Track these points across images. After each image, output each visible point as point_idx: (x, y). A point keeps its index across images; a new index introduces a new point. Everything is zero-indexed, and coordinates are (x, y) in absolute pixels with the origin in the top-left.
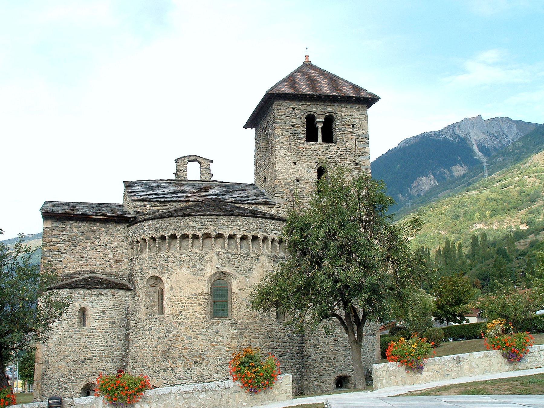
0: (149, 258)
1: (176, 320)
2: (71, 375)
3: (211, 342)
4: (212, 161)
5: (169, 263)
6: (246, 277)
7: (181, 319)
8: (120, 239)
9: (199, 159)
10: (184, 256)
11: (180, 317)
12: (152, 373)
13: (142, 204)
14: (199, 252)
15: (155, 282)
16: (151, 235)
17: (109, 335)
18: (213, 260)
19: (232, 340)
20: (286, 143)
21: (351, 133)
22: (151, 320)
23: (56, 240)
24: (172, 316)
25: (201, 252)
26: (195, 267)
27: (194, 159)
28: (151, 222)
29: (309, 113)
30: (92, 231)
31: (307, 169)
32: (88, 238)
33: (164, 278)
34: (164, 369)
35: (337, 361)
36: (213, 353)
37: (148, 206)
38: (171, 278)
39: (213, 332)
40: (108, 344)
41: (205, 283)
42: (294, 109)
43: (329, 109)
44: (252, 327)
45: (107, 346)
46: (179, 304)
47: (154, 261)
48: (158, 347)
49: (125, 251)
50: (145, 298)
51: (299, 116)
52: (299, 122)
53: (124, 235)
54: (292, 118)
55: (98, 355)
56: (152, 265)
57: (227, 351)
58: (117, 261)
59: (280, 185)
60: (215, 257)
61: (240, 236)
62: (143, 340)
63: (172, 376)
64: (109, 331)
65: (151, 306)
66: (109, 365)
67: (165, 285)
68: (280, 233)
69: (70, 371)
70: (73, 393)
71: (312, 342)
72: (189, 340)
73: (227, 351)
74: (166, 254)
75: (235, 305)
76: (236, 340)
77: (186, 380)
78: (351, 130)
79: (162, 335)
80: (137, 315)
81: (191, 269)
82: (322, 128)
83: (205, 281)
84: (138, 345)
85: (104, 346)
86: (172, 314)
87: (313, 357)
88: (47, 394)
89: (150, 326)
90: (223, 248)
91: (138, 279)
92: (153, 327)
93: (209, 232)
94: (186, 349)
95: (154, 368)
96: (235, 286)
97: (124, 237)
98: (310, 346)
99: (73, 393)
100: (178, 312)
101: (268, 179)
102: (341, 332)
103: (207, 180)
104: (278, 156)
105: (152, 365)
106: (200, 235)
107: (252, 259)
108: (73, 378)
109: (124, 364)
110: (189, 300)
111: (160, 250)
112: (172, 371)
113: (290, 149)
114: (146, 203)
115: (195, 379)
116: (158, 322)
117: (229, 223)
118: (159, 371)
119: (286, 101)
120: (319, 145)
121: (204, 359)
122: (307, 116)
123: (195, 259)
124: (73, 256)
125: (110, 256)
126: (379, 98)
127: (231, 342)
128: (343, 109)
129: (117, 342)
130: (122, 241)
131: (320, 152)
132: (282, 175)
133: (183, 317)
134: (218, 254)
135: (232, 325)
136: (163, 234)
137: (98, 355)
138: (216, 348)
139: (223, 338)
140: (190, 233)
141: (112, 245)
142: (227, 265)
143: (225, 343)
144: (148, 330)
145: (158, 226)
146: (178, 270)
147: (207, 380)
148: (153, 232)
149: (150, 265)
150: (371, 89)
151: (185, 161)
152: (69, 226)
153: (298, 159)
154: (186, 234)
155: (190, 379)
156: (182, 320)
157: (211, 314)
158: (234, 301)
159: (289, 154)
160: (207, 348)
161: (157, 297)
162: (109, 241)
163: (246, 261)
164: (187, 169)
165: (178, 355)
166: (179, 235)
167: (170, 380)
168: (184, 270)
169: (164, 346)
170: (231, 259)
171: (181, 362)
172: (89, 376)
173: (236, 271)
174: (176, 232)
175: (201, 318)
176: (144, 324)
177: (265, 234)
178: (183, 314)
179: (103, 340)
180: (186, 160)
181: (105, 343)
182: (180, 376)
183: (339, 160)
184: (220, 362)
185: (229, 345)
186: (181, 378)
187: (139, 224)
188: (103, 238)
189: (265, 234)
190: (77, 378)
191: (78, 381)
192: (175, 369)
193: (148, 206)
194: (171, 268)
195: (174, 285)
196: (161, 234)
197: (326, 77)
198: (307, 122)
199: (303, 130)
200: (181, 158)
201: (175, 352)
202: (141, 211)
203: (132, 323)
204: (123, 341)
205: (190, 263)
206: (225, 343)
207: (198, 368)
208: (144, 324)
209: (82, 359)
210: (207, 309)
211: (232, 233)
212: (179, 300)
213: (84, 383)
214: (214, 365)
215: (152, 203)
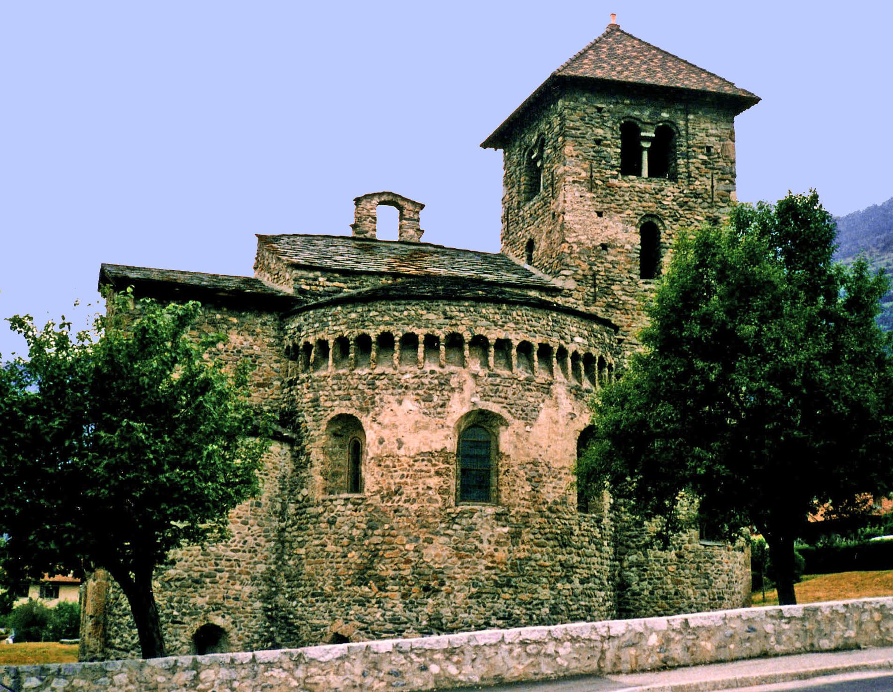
0: (333, 379)
1: (389, 504)
2: (172, 607)
3: (457, 549)
4: (422, 207)
5: (376, 391)
7: (399, 501)
8: (267, 340)
9: (401, 203)
10: (408, 376)
12: (334, 609)
13: (311, 275)
14: (438, 369)
15: (343, 428)
16: (340, 333)
17: (249, 529)
18: (465, 387)
20: (584, 174)
21: (704, 162)
22: (335, 503)
24: (378, 497)
25: (441, 370)
26: (428, 399)
27: (393, 200)
28: (339, 308)
29: (627, 120)
31: (621, 226)
33: (365, 420)
34: (361, 601)
35: (682, 598)
36: (460, 571)
37: (321, 279)
38: (379, 419)
39: (463, 529)
40: (246, 548)
41: (449, 433)
42: (600, 110)
43: (665, 115)
44: (536, 521)
45: (244, 551)
46: (396, 471)
47: (345, 384)
48: (349, 555)
49: (275, 366)
50: (322, 458)
51: (609, 124)
52: (609, 136)
53: (274, 333)
54: (597, 127)
55: (227, 569)
56: (341, 392)
57: (488, 568)
58: (259, 385)
59: (571, 253)
60: (470, 383)
61: (516, 343)
62: (317, 542)
63: (378, 615)
64: (251, 521)
66: (247, 590)
67: (367, 433)
68: (586, 342)
69: (171, 600)
70: (175, 643)
71: (633, 558)
72: (414, 544)
73: (488, 568)
74: (370, 371)
75: (505, 479)
76: (506, 548)
77: (406, 623)
78: (705, 158)
79: (355, 532)
80: (304, 492)
81: (423, 403)
82: (649, 150)
83: (448, 427)
84: (302, 551)
85: (239, 551)
86: (379, 492)
87: (635, 587)
88: (120, 644)
89: (332, 514)
90: (485, 364)
91: (306, 419)
93: (460, 332)
94: (408, 561)
95: (339, 599)
96: (506, 440)
97: (274, 337)
98: (630, 567)
99: (175, 643)
101: (542, 245)
102: (690, 542)
103: (412, 241)
104: (569, 197)
105: (335, 593)
106: (442, 337)
107: (538, 390)
108: (175, 613)
109: (274, 589)
110: (416, 464)
111: (357, 364)
112: (376, 605)
113: (591, 185)
114: (318, 273)
115: (424, 623)
116: (350, 506)
117: (498, 317)
118: (349, 605)
119: (587, 95)
120: (642, 182)
121: (442, 584)
122: (622, 125)
123: (430, 383)
126: (760, 99)
127: (496, 550)
128: (691, 117)
129: (263, 543)
130: (270, 345)
131: (647, 196)
132: (574, 234)
133: (404, 498)
134: (475, 376)
135: (498, 517)
136: (366, 331)
137: (227, 569)
138: (468, 562)
139: (481, 542)
140: (421, 333)
141: (251, 351)
142: (493, 399)
143: (485, 553)
145: (353, 315)
147: (449, 625)
148: (343, 327)
149: (337, 393)
150: (743, 83)
151: (374, 202)
153: (606, 206)
154: (413, 334)
155: (415, 622)
156: (400, 503)
157: (458, 493)
158: (503, 470)
159: (589, 195)
160: (449, 561)
161: (344, 459)
162: (245, 343)
163: (527, 393)
164: (375, 218)
165: (391, 573)
166: (398, 335)
167: (372, 623)
168: (409, 403)
169: (361, 556)
170: (500, 388)
171: (397, 588)
172: (207, 612)
173: (509, 412)
174: (392, 328)
175: (440, 499)
176: (321, 509)
177: (562, 342)
179: (238, 540)
180: (376, 201)
181: (241, 544)
182: (394, 615)
183: (681, 212)
184: (474, 590)
185: (492, 556)
186: (395, 620)
187: (311, 312)
188: (235, 339)
189: (562, 342)
190: (184, 614)
191: (186, 619)
192: (383, 600)
193: (321, 279)
194: (381, 400)
195: (386, 433)
197: (654, 55)
198: (622, 138)
199: (614, 151)
200: (366, 196)
201: (384, 569)
202: (308, 288)
203: (292, 509)
204: (272, 544)
205: (421, 392)
206: (485, 553)
207: (430, 601)
208: (321, 509)
209: (196, 575)
210: (453, 483)
211: (502, 336)
212: (397, 464)
213: (198, 625)
214: (461, 595)
215: (329, 274)
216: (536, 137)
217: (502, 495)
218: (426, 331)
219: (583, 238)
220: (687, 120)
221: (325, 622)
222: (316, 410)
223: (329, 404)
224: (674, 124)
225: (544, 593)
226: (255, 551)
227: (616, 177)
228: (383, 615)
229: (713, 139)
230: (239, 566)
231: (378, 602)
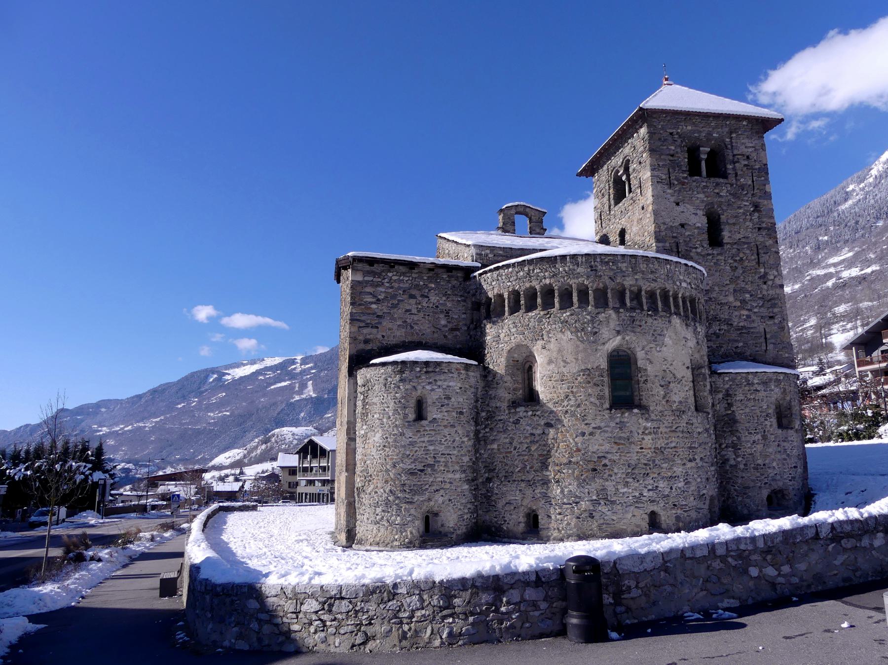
1: (560, 409)
6: (657, 345)
11: (566, 403)
19: (645, 437)
21: (745, 165)
23: (369, 299)
30: (417, 287)
32: (412, 297)
40: (456, 444)
42: (671, 134)
49: (464, 316)
65: (514, 390)
66: (458, 476)
73: (637, 452)
82: (707, 161)
84: (495, 446)
97: (461, 296)
114: (488, 251)
120: (702, 181)
124: (393, 319)
125: (443, 322)
146: (560, 335)
152: (386, 280)
156: (568, 408)
158: (642, 380)
159: (669, 191)
164: (514, 223)
180: (513, 212)
196: (528, 285)
199: (683, 159)
216: (621, 160)
217: (644, 400)
218: (576, 281)
219: (668, 220)
223: (507, 339)
224: (724, 141)
225: (679, 470)
226: (461, 447)
227: (686, 178)
228: (562, 492)
229: (750, 150)
230: (451, 458)
231: (558, 482)
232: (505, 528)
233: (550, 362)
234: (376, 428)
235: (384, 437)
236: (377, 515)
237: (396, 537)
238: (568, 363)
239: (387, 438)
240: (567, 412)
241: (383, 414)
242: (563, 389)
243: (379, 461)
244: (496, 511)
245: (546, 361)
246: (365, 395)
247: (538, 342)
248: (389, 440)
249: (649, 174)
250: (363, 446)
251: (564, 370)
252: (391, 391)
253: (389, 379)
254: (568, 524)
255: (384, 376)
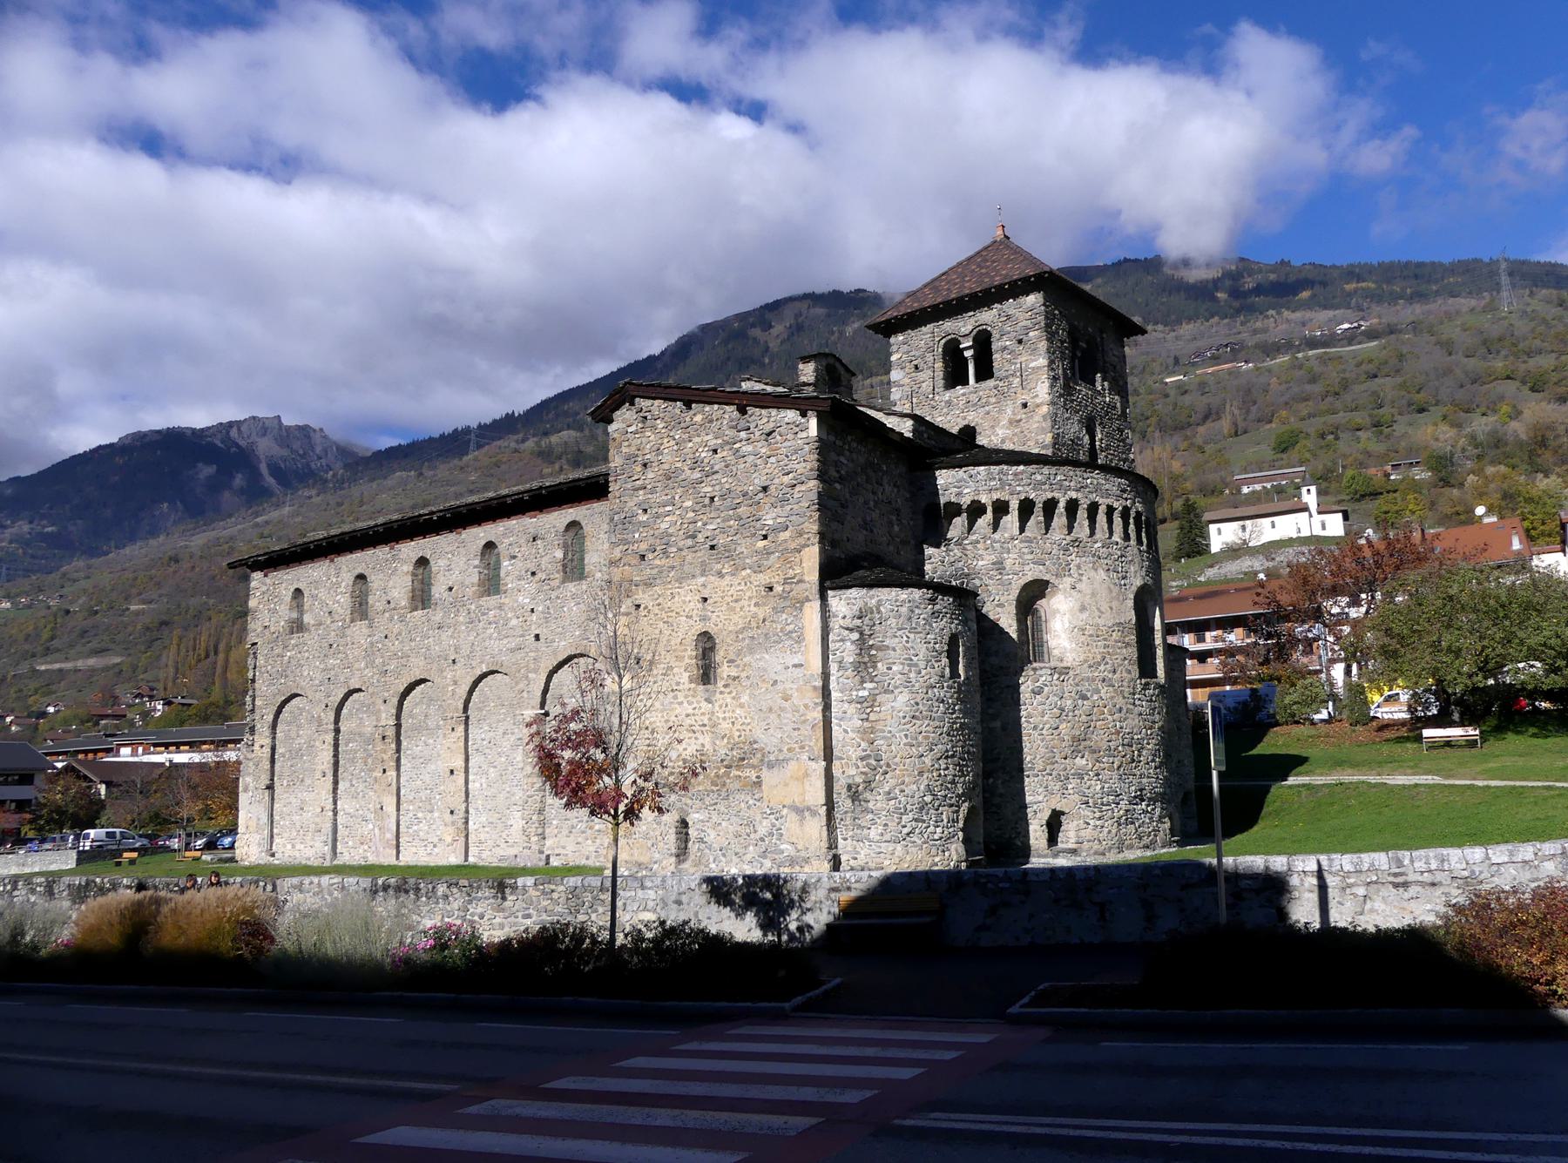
0: (1021, 542)
1: (1096, 674)
11: (1102, 668)
24: (1086, 665)
28: (1022, 467)
86: (1086, 661)
92: (1046, 685)
100: (1099, 657)
144: (1033, 691)
145: (1039, 477)
146: (1092, 573)
178: (1107, 663)
187: (982, 468)
216: (971, 328)
220: (1102, 338)
221: (1040, 798)
222: (1001, 574)
232: (1019, 844)
233: (1083, 609)
234: (896, 687)
235: (912, 702)
236: (904, 827)
237: (937, 859)
238: (1102, 613)
239: (917, 704)
240: (1104, 680)
241: (909, 665)
242: (1098, 650)
243: (905, 741)
244: (999, 820)
245: (1077, 606)
246: (867, 632)
247: (1064, 579)
248: (920, 706)
249: (1042, 361)
250: (865, 716)
251: (1099, 621)
252: (919, 630)
253: (917, 611)
254: (1109, 832)
255: (907, 605)
